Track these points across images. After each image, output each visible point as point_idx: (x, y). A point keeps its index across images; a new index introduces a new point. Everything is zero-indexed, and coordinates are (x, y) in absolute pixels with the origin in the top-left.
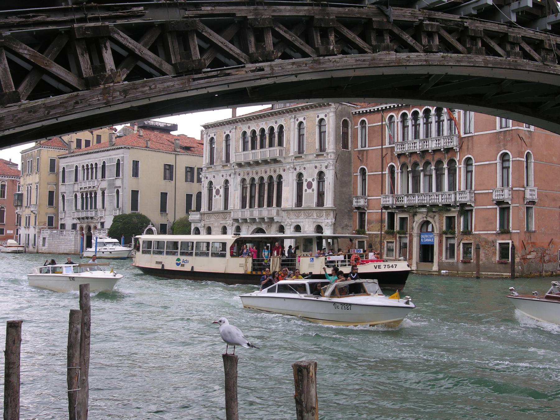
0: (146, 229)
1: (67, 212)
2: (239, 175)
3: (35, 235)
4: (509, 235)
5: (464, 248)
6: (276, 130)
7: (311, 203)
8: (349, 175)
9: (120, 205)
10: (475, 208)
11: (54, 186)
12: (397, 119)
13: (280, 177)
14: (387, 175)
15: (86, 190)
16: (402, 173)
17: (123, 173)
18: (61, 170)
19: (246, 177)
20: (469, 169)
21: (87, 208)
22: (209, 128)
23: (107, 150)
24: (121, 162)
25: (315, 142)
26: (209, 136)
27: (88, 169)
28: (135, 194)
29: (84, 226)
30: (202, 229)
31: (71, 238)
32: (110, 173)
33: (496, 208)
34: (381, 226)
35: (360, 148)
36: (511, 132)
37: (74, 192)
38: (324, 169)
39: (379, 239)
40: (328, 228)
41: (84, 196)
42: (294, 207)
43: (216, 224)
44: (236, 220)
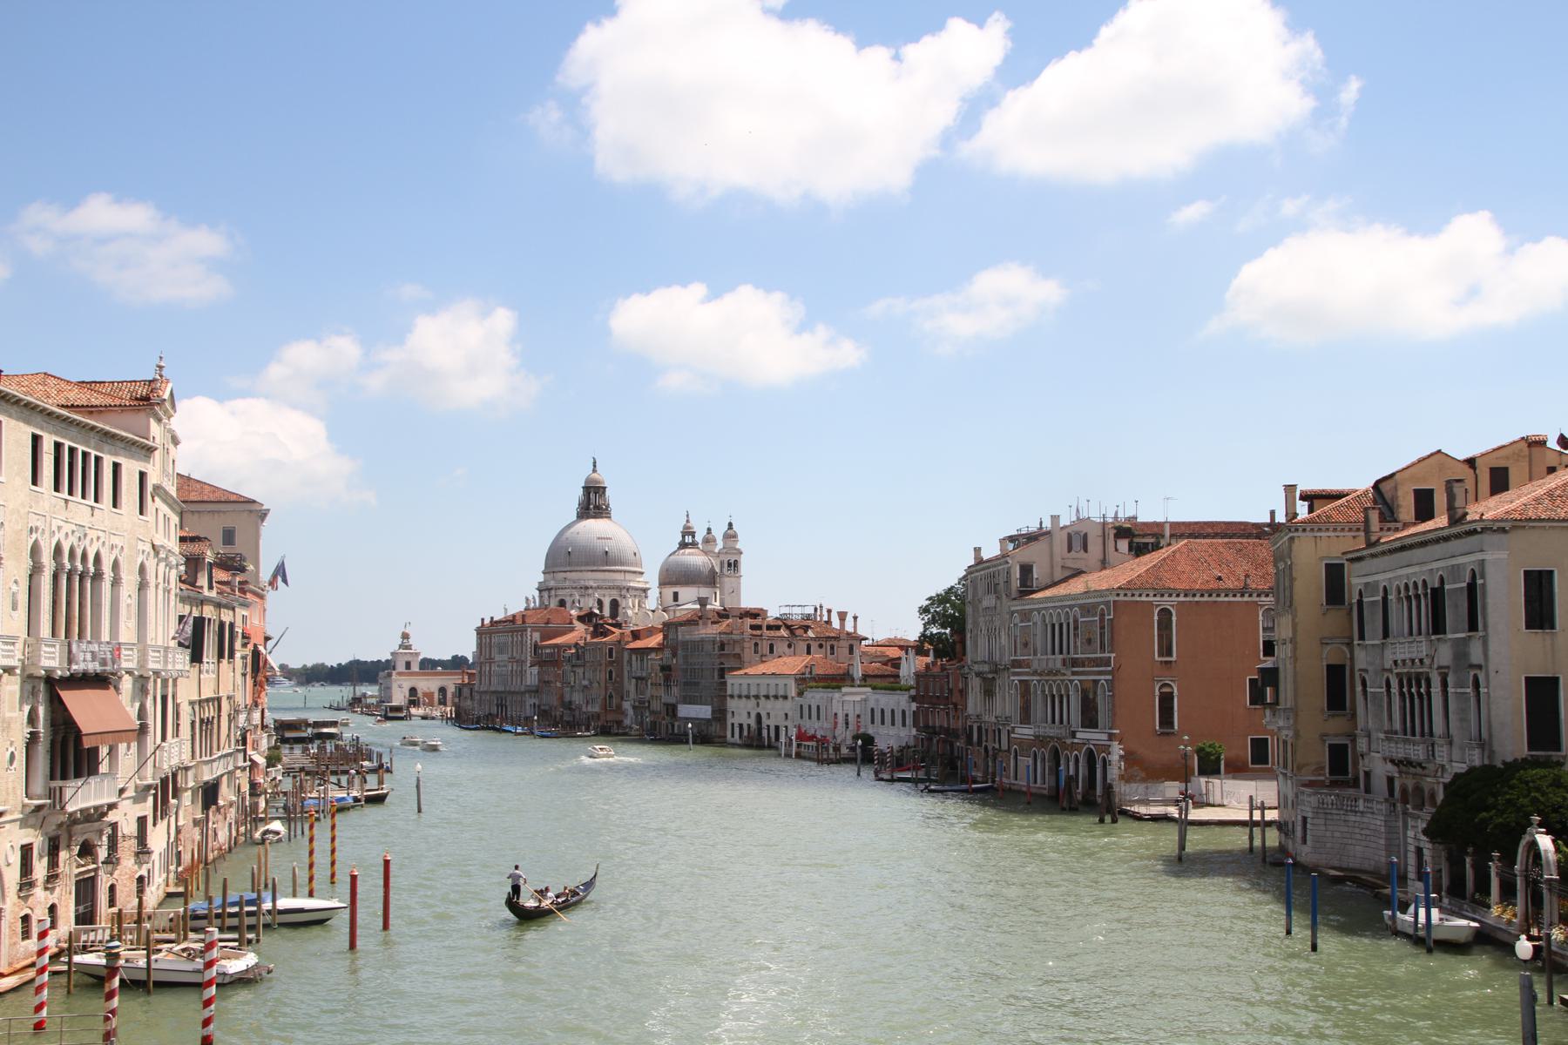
0: (1523, 843)
1: (1374, 735)
3: (1293, 801)
9: (1485, 735)
11: (1345, 648)
15: (1405, 670)
17: (1484, 618)
18: (1355, 601)
21: (1413, 734)
23: (1446, 539)
24: (1479, 582)
27: (1408, 598)
28: (1541, 692)
29: (1410, 783)
31: (1379, 823)
32: (1455, 613)
37: (1384, 670)
41: (1405, 690)
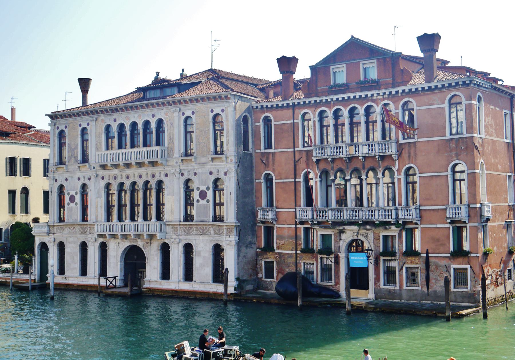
2: (103, 178)
4: (466, 259)
5: (407, 272)
6: (153, 126)
7: (206, 217)
8: (252, 181)
10: (421, 226)
12: (314, 117)
13: (160, 183)
14: (302, 184)
16: (321, 181)
19: (112, 181)
20: (411, 179)
22: (57, 118)
25: (209, 143)
26: (58, 128)
30: (52, 244)
33: (449, 228)
34: (296, 243)
35: (263, 150)
36: (465, 140)
38: (221, 176)
39: (293, 260)
40: (231, 247)
42: (182, 220)
43: (71, 239)
44: (101, 236)
